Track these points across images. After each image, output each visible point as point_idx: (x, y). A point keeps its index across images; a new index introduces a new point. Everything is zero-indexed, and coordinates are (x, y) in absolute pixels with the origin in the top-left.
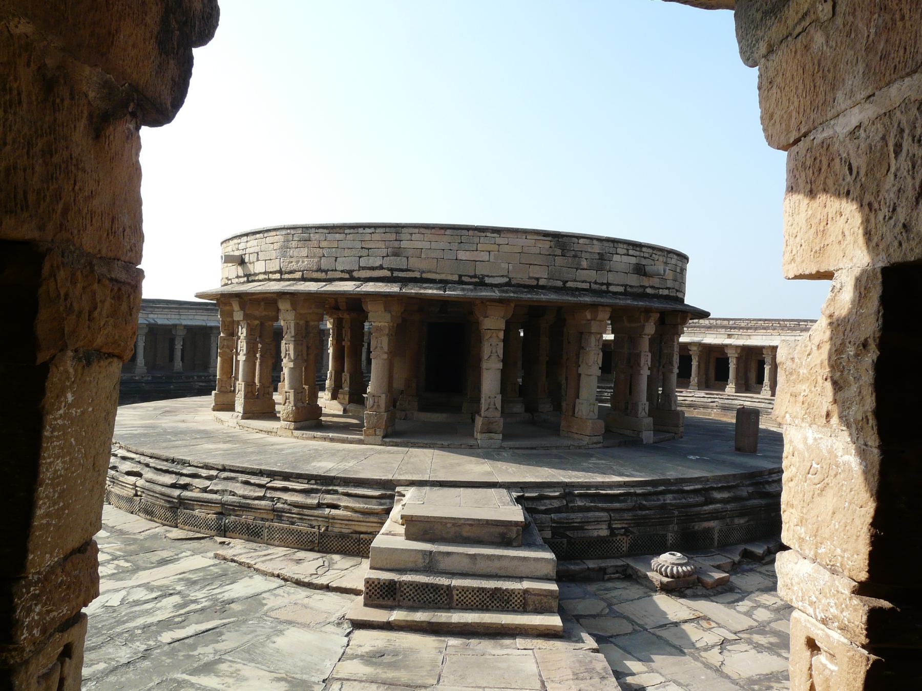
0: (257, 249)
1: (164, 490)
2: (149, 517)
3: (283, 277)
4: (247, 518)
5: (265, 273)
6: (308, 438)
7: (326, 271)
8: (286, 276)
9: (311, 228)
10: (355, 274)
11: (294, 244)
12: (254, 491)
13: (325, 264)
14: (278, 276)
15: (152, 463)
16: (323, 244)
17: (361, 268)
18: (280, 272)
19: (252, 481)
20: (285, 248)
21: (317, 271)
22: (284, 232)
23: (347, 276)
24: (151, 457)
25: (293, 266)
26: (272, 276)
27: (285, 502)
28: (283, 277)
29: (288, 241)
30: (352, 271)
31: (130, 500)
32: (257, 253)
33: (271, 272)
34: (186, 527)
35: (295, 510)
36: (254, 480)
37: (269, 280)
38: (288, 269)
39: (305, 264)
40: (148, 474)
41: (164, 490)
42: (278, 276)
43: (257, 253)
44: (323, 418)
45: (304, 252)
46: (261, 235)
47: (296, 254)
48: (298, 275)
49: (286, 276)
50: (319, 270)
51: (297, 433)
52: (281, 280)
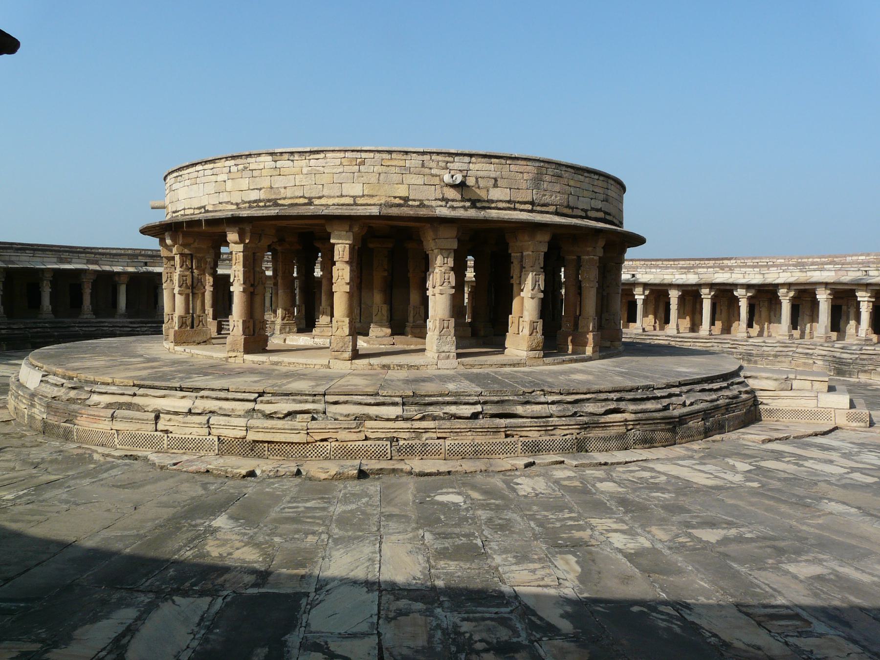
0: (493, 175)
1: (661, 414)
2: (647, 446)
3: (535, 208)
4: (718, 416)
5: (509, 202)
6: (558, 363)
7: (572, 208)
8: (539, 208)
9: (563, 165)
10: (590, 214)
11: (548, 178)
12: (710, 395)
13: (572, 201)
14: (529, 207)
15: (630, 396)
16: (572, 183)
17: (593, 209)
18: (532, 203)
19: (707, 388)
20: (537, 181)
21: (566, 207)
22: (537, 164)
23: (584, 214)
24: (610, 392)
25: (547, 199)
26: (517, 206)
27: (728, 397)
28: (535, 208)
29: (542, 174)
30: (585, 211)
31: (621, 437)
32: (496, 180)
33: (519, 202)
34: (684, 441)
35: (735, 401)
36: (707, 386)
37: (515, 209)
38: (542, 202)
39: (557, 199)
40: (632, 407)
41: (661, 414)
42: (529, 207)
43: (496, 180)
44: (808, 325)
45: (557, 188)
46: (503, 161)
47: (549, 188)
48: (552, 209)
49: (539, 208)
50: (568, 207)
51: (548, 360)
52: (531, 211)
